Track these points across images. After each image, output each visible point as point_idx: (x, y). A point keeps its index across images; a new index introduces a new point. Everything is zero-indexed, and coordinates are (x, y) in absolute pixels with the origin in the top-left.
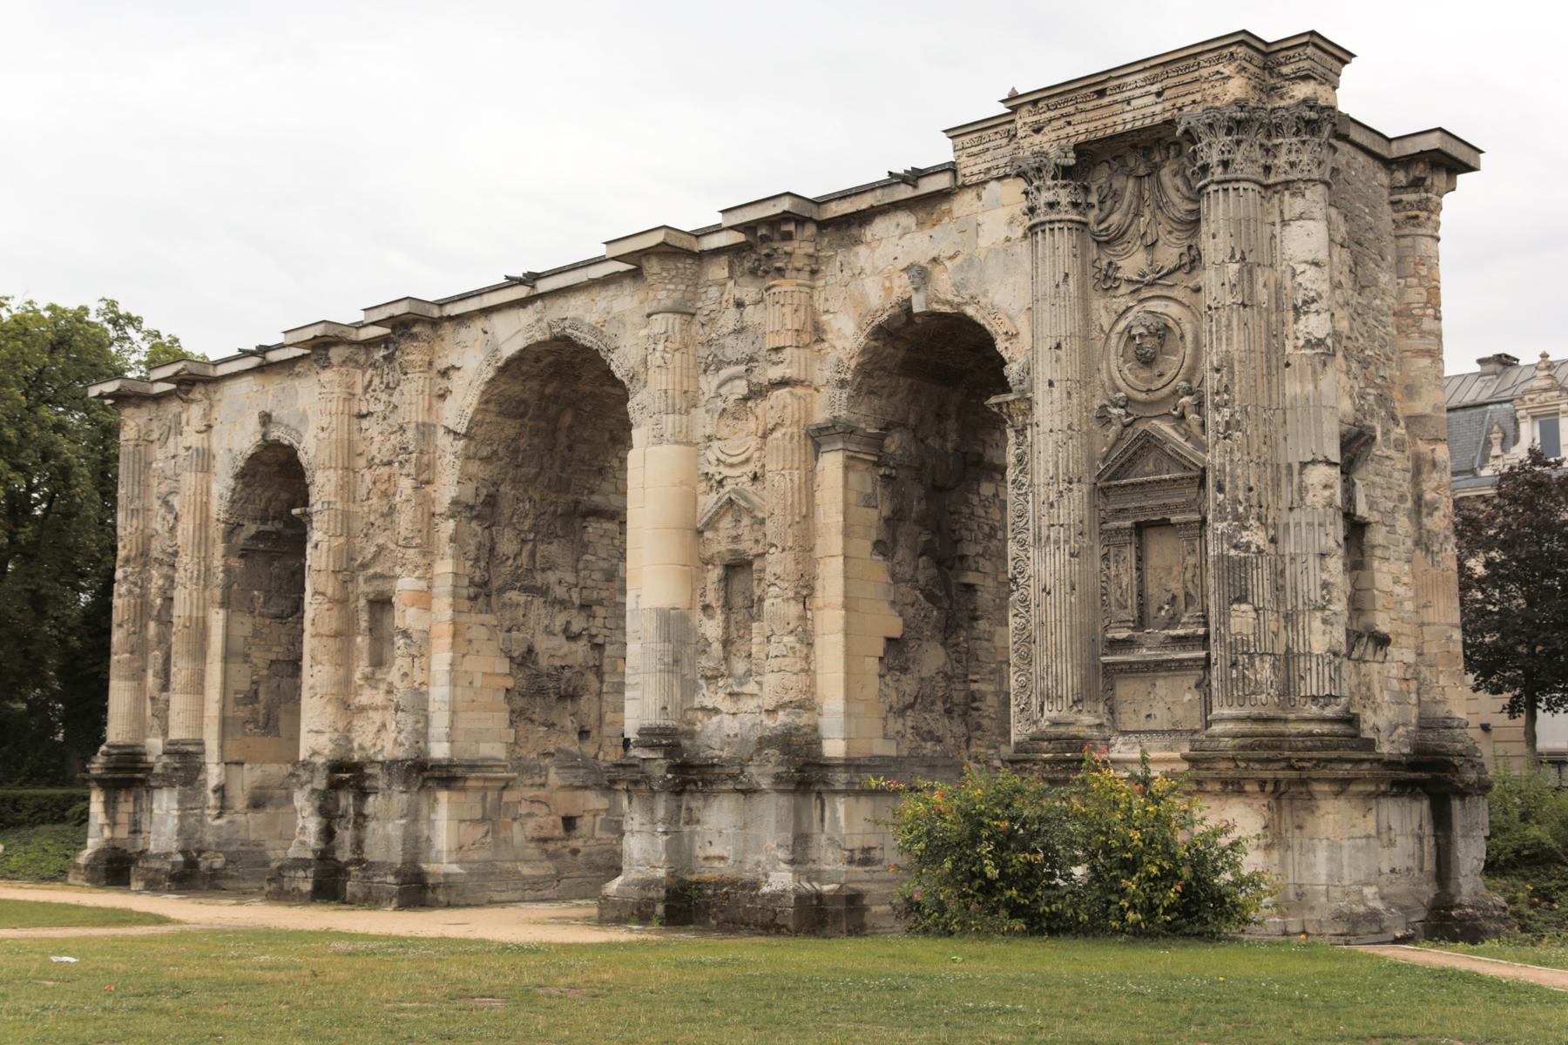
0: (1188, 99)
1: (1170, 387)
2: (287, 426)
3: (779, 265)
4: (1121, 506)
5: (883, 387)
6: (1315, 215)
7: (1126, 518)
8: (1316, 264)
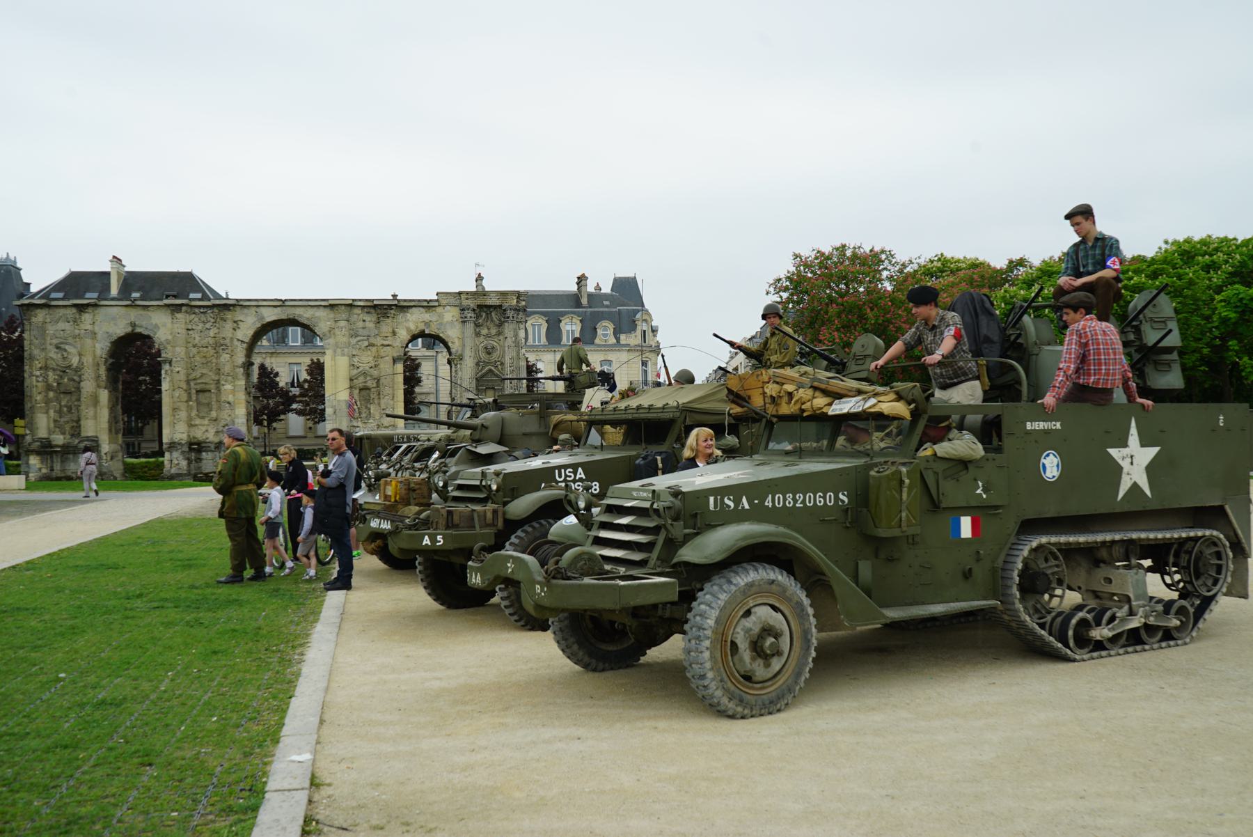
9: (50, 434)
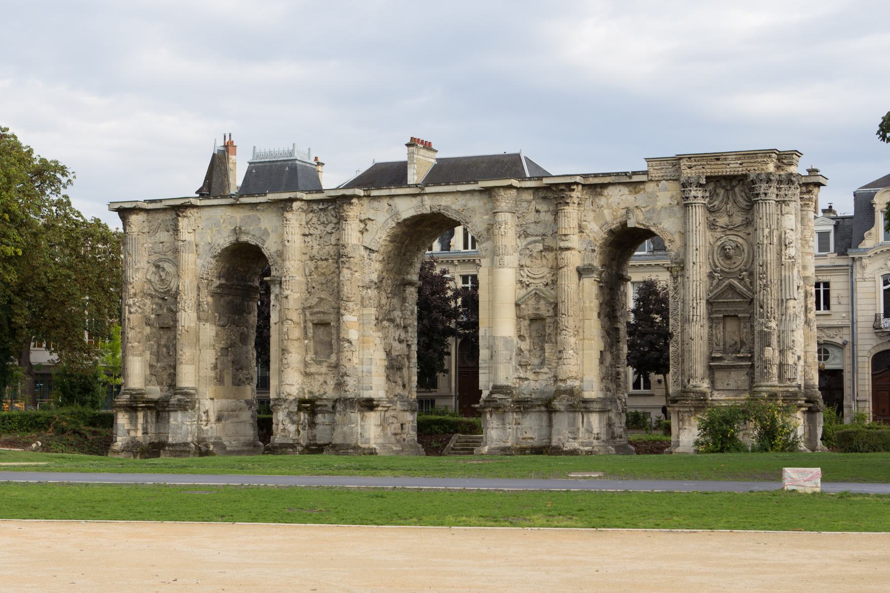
0: (752, 168)
2: (254, 236)
3: (567, 201)
4: (719, 309)
7: (720, 314)
8: (792, 230)
9: (146, 385)
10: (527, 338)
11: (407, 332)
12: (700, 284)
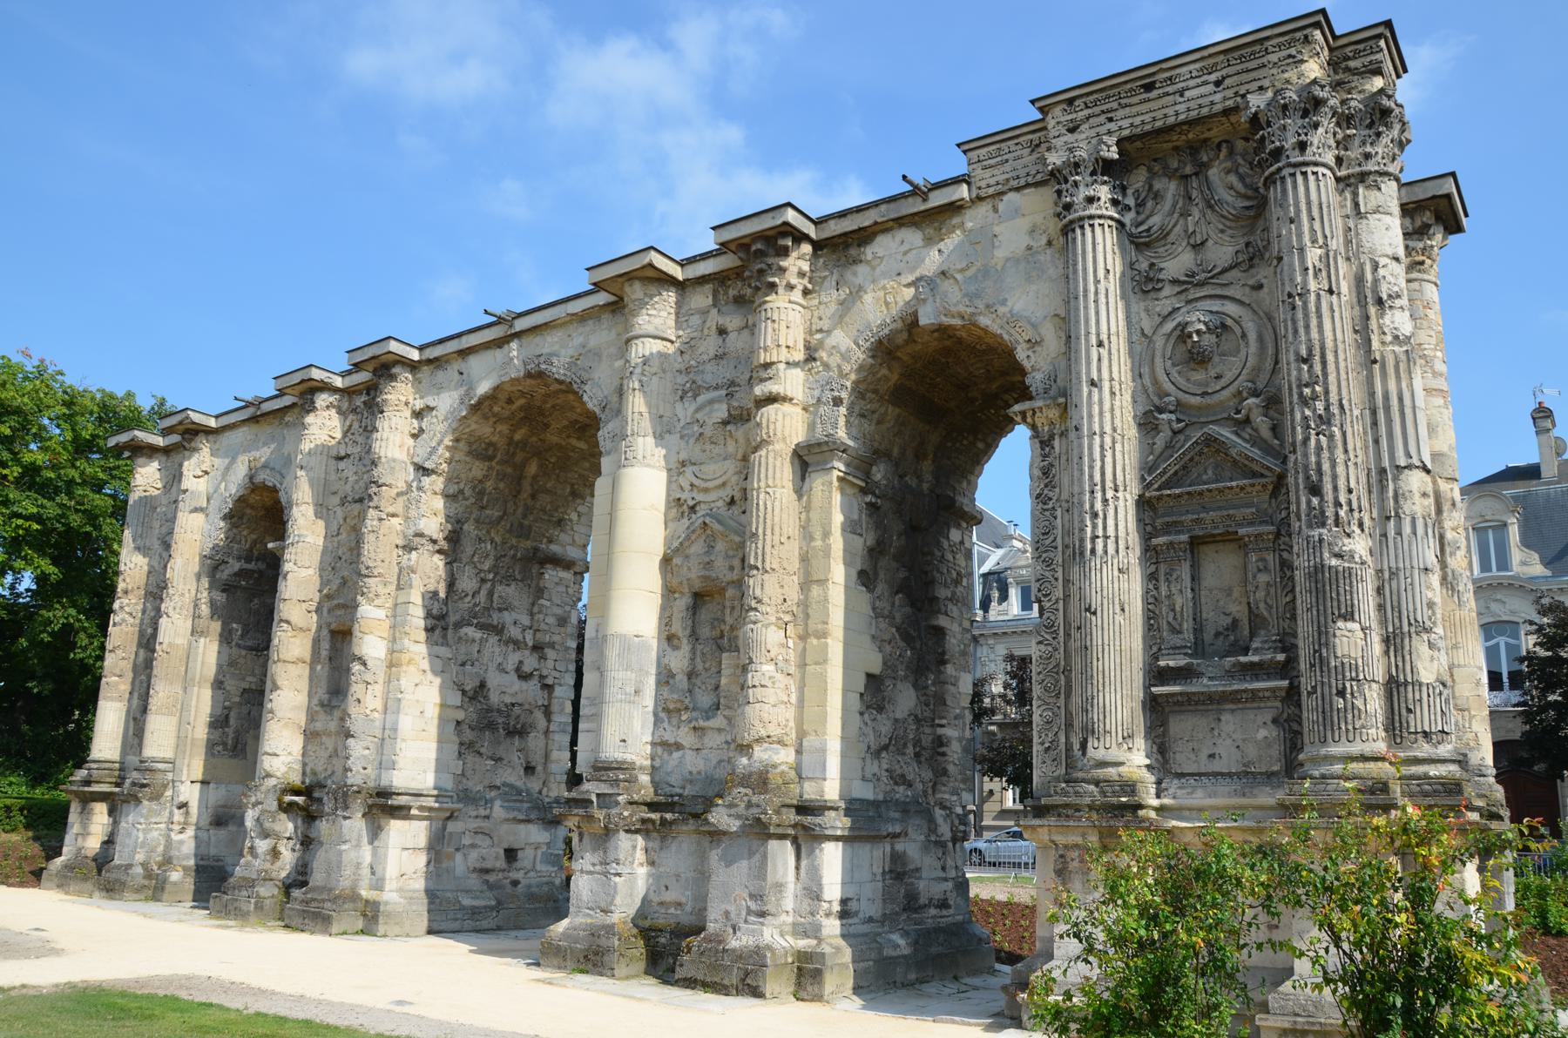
0: (1255, 85)
1: (1232, 389)
3: (771, 280)
4: (1174, 518)
5: (873, 412)
6: (1390, 210)
7: (1179, 532)
8: (1397, 259)
10: (685, 641)
11: (543, 658)
12: (1114, 442)
